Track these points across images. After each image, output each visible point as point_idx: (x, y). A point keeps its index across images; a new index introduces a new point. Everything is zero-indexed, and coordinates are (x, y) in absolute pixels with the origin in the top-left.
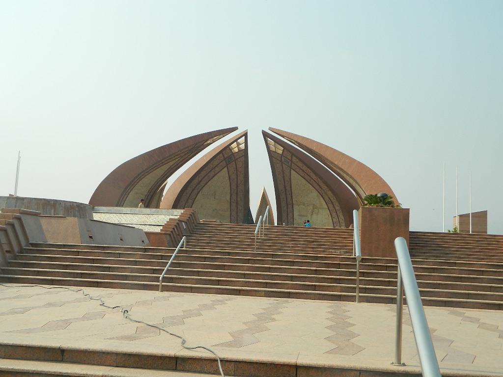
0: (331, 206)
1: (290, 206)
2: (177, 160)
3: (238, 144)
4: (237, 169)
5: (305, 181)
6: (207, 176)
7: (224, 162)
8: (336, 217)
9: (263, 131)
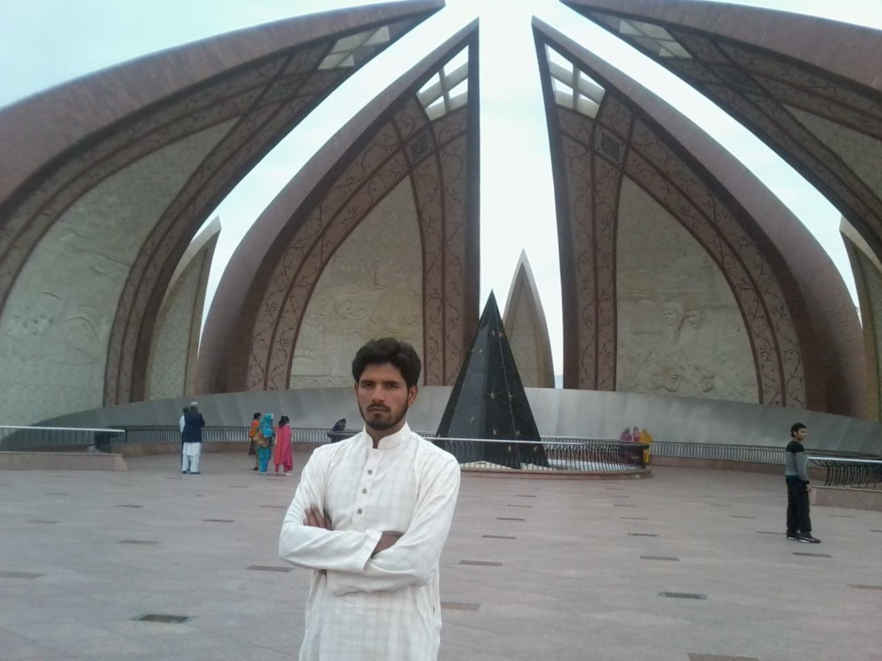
0: (754, 295)
1: (606, 305)
2: (226, 127)
3: (445, 86)
4: (442, 182)
5: (666, 216)
6: (345, 211)
7: (400, 156)
8: (768, 334)
9: (534, 18)
